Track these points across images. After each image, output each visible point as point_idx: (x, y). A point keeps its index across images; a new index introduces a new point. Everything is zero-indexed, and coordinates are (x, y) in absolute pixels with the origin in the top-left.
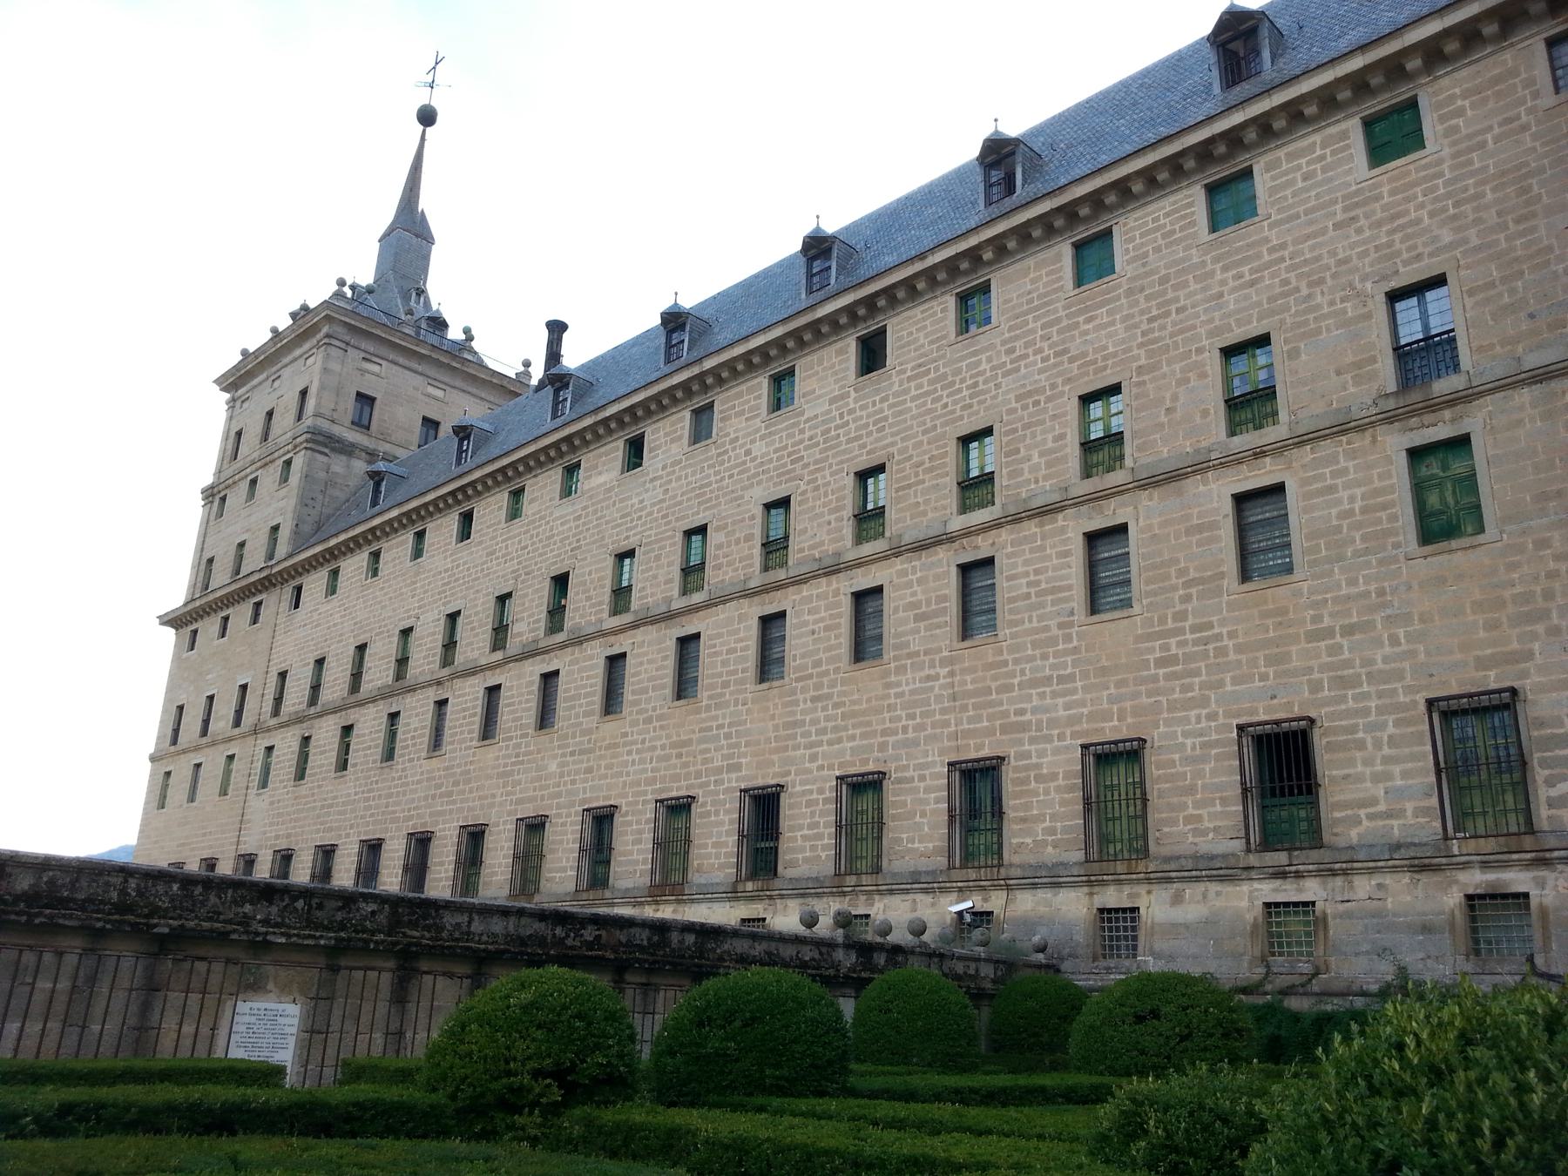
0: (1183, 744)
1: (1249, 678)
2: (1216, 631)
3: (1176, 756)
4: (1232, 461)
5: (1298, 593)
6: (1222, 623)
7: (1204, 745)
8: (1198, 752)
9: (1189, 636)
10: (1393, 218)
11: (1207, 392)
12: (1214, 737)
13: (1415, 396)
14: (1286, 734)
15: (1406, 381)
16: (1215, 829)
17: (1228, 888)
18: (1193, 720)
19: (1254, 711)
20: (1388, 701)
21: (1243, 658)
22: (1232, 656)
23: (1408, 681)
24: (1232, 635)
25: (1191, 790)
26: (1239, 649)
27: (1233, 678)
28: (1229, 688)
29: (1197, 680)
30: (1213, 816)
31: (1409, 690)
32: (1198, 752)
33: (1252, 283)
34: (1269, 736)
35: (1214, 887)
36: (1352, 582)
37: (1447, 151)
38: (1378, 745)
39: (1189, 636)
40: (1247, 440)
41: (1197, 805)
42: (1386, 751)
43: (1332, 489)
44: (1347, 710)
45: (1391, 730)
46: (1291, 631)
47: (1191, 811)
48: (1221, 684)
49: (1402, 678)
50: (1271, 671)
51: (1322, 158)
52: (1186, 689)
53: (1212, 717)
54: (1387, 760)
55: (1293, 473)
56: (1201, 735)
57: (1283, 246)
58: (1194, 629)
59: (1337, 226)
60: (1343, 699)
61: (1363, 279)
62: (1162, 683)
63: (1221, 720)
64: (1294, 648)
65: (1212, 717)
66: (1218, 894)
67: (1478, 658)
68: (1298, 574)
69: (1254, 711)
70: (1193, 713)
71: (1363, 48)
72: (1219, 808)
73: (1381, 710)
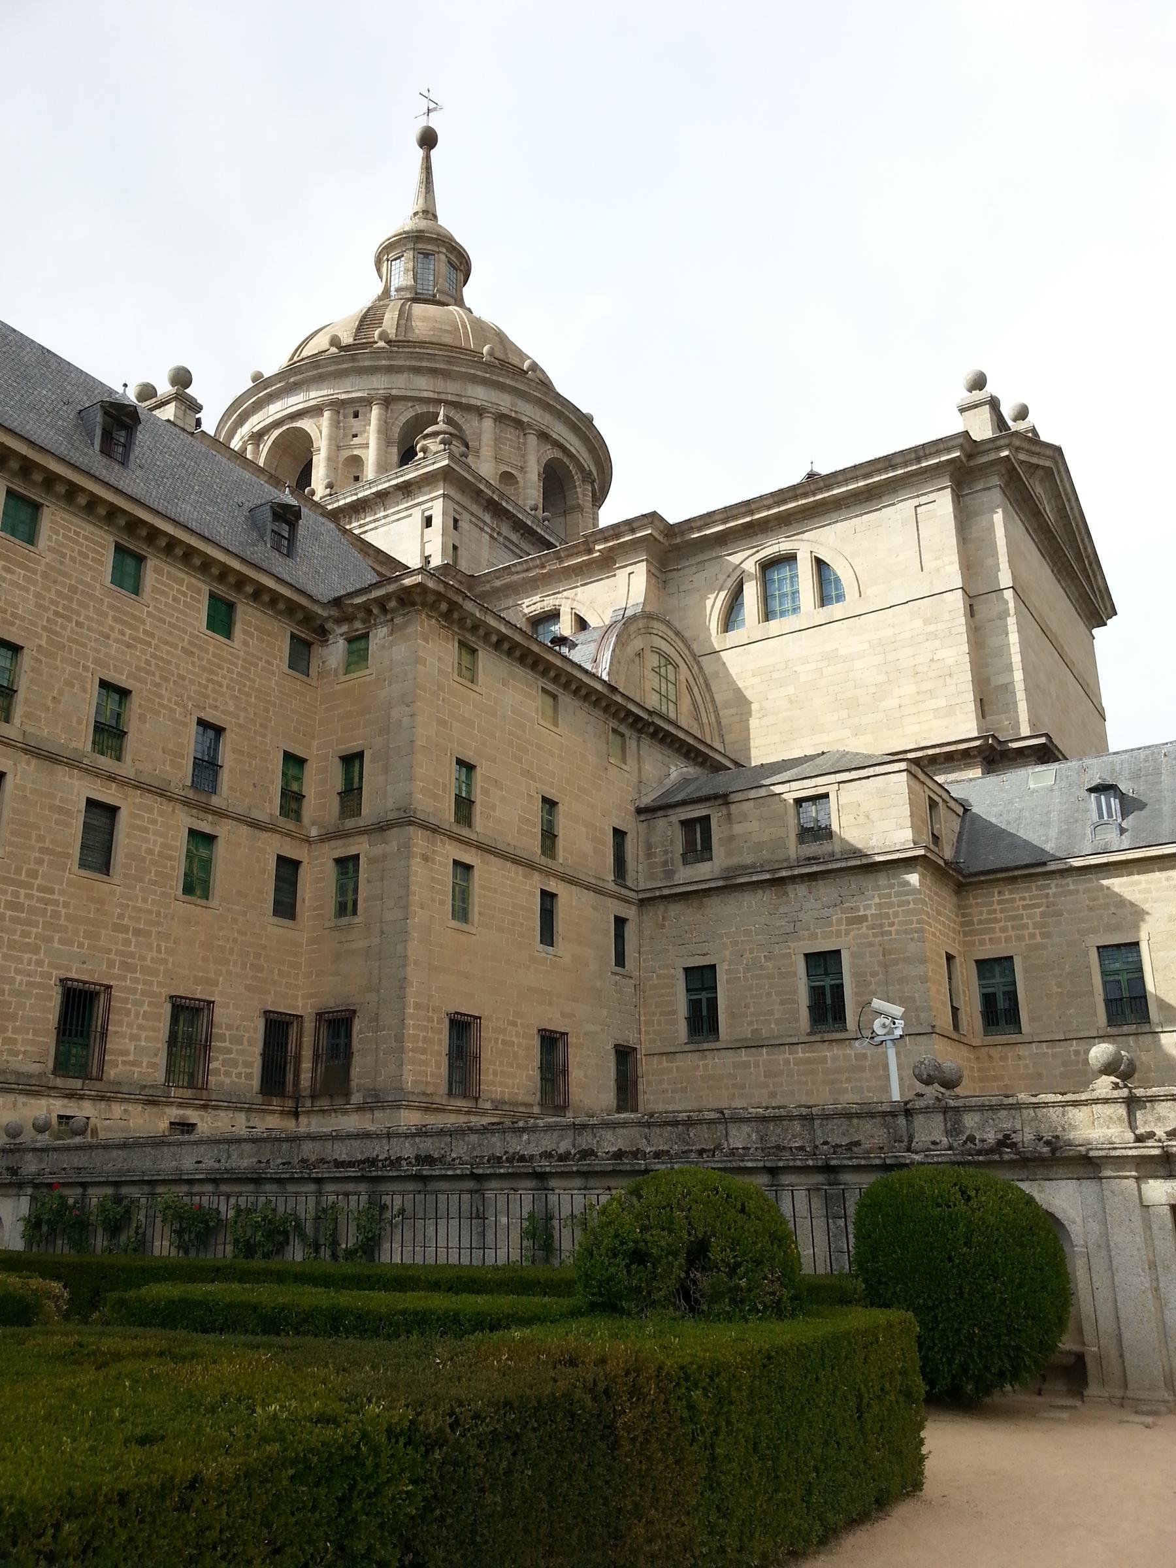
0: (14, 979)
1: (71, 943)
2: (55, 897)
3: (7, 987)
5: (113, 893)
6: (62, 893)
7: (29, 984)
8: (24, 988)
9: (35, 893)
12: (38, 980)
14: (86, 992)
16: (25, 1053)
17: (32, 1101)
18: (25, 961)
19: (68, 969)
20: (147, 987)
21: (70, 926)
22: (63, 922)
23: (161, 978)
24: (66, 905)
25: (13, 1017)
26: (68, 917)
27: (60, 938)
28: (56, 945)
29: (34, 930)
30: (25, 1042)
31: (160, 984)
32: (24, 988)
34: (75, 990)
35: (22, 1099)
38: (137, 1016)
39: (35, 893)
41: (16, 1030)
42: (140, 1021)
44: (126, 987)
45: (146, 1007)
46: (104, 918)
47: (9, 1034)
48: (50, 940)
49: (158, 976)
50: (86, 942)
52: (25, 934)
53: (40, 963)
54: (140, 1027)
55: (129, 805)
56: (29, 975)
58: (41, 889)
60: (124, 979)
61: (189, 698)
62: (7, 923)
63: (46, 969)
64: (103, 932)
65: (40, 963)
66: (24, 1104)
67: (195, 976)
69: (68, 969)
70: (27, 956)
71: (244, 561)
72: (30, 1037)
73: (143, 993)
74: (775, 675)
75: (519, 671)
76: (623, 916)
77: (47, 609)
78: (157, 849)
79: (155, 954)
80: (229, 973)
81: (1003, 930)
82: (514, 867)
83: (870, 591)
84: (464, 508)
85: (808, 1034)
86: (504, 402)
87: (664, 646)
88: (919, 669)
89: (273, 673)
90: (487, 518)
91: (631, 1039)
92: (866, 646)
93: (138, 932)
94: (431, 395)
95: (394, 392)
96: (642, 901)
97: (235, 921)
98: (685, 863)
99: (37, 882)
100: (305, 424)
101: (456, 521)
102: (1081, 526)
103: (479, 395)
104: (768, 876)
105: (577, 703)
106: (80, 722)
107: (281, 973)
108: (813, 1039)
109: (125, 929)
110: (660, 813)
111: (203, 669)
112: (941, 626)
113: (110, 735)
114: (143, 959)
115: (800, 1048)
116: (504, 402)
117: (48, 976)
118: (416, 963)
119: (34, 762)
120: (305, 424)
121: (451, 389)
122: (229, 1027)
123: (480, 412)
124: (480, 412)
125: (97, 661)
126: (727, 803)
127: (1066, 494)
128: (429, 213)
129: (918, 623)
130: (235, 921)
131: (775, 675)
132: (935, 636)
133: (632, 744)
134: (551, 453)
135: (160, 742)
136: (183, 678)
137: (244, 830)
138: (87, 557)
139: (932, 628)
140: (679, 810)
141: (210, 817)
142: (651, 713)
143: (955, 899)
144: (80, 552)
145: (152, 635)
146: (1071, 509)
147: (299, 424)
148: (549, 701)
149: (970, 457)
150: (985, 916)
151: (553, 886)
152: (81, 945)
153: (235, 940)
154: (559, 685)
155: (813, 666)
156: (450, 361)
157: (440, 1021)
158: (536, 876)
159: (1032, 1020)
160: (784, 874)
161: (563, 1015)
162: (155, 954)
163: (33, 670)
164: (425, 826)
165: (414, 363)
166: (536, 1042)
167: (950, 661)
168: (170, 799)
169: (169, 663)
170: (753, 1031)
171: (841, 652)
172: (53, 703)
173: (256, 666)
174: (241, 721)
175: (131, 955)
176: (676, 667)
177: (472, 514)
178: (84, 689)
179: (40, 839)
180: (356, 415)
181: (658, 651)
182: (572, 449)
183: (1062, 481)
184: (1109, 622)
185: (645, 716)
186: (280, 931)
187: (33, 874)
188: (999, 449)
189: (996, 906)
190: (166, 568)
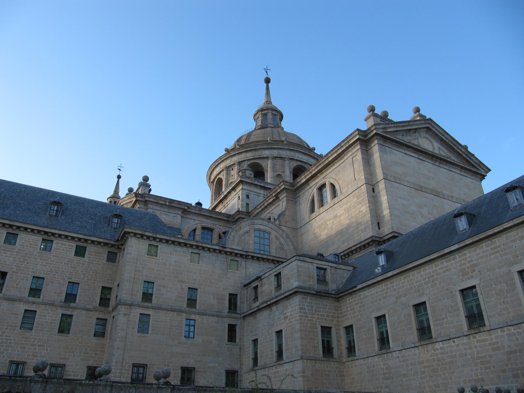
4: (29, 302)
10: (75, 268)
11: (27, 285)
13: (67, 304)
15: (66, 301)
22: (13, 345)
24: (14, 340)
33: (45, 266)
36: (43, 336)
37: (87, 261)
40: (31, 299)
43: (46, 316)
48: (8, 350)
51: (67, 248)
57: (53, 261)
59: (65, 263)
60: (33, 359)
63: (5, 358)
68: (33, 331)
74: (323, 227)
75: (178, 248)
76: (234, 323)
77: (16, 261)
78: (49, 321)
79: (45, 352)
80: (74, 355)
81: (350, 314)
82: (172, 313)
83: (344, 191)
84: (251, 191)
85: (276, 362)
86: (275, 153)
87: (262, 227)
88: (357, 215)
89: (100, 264)
90: (262, 192)
91: (236, 367)
92: (344, 211)
93: (39, 346)
94: (252, 158)
95: (241, 160)
96: (243, 317)
97: (78, 339)
98: (255, 302)
99: (5, 335)
100: (220, 176)
101: (248, 197)
102: (455, 143)
103: (266, 153)
104: (265, 305)
105: (210, 254)
106: (25, 289)
107: (96, 354)
108: (276, 364)
109: (35, 345)
110: (249, 286)
111: (72, 268)
112: (361, 199)
113: (35, 292)
114: (41, 353)
115: (274, 368)
116: (275, 153)
117: (7, 360)
118: (118, 349)
119: (7, 302)
120: (220, 176)
121: (257, 154)
122: (72, 372)
123: (267, 158)
124: (267, 158)
125: (32, 272)
126: (261, 280)
127: (441, 134)
128: (269, 102)
129: (356, 199)
130: (78, 339)
131: (323, 227)
132: (360, 203)
133: (243, 263)
134: (295, 164)
135: (54, 291)
136: (63, 271)
137: (84, 312)
138: (32, 244)
139: (359, 200)
140: (252, 284)
141: (71, 310)
142: (247, 252)
143: (336, 304)
144: (30, 244)
145: (53, 261)
146: (446, 138)
147: (218, 177)
148: (197, 256)
149: (366, 136)
150: (346, 309)
151: (193, 317)
152: (18, 351)
153: (77, 345)
154: (200, 250)
155: (331, 221)
156: (255, 146)
157: (128, 366)
158: (184, 315)
159: (359, 350)
160: (269, 303)
161: (195, 361)
162: (45, 352)
163: (10, 277)
164: (125, 304)
165: (245, 150)
166: (180, 372)
167: (364, 211)
168: (55, 306)
169: (59, 268)
170: (265, 362)
171: (338, 215)
172: (18, 285)
173: (93, 263)
174: (86, 280)
175: (37, 352)
176: (269, 233)
177: (255, 192)
178: (27, 280)
179: (7, 323)
180: (233, 169)
181: (255, 230)
182: (304, 161)
183: (436, 130)
184: (488, 174)
185: (245, 253)
186: (96, 341)
187: (4, 332)
188: (372, 131)
189: (348, 305)
190: (60, 242)
